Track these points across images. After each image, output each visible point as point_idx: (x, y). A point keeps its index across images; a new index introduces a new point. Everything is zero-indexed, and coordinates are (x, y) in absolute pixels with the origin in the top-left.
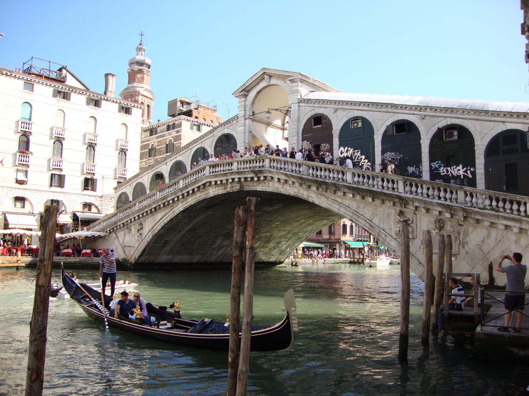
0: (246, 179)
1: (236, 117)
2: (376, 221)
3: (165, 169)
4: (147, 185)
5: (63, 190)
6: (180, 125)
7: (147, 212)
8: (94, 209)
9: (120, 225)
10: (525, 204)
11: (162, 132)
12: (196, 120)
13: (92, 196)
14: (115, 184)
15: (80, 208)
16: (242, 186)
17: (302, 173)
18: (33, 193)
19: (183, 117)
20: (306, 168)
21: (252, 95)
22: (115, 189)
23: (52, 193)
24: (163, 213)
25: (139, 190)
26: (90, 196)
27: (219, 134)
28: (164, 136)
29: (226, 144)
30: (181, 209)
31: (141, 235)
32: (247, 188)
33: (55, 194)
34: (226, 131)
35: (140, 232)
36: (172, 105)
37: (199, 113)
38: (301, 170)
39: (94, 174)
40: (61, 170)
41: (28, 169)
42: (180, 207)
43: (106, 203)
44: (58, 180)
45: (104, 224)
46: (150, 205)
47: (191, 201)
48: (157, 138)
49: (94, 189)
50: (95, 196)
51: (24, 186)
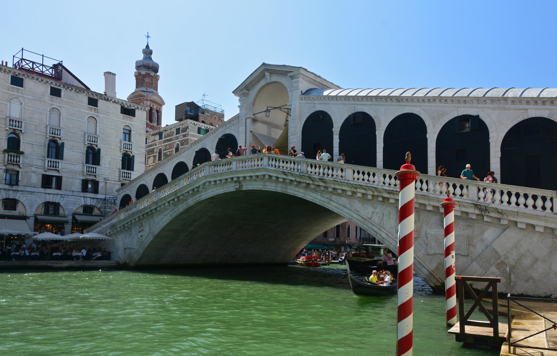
0: (245, 177)
1: (237, 117)
2: (376, 219)
3: (168, 170)
4: (150, 186)
7: (147, 213)
8: (96, 211)
9: (120, 227)
10: (551, 199)
11: (168, 136)
12: (203, 124)
13: (94, 198)
14: (118, 186)
16: (241, 186)
17: (299, 171)
18: (26, 195)
19: (189, 121)
20: (305, 165)
22: (118, 191)
23: (48, 196)
25: (142, 191)
26: (91, 198)
27: (220, 136)
28: (171, 140)
29: (227, 145)
31: (141, 236)
33: (51, 196)
34: (228, 132)
35: (140, 234)
36: (179, 108)
38: (299, 167)
39: (95, 176)
40: (58, 171)
41: (20, 171)
43: (110, 205)
45: (104, 226)
46: (149, 206)
47: (191, 202)
48: (164, 142)
49: (96, 190)
50: (97, 199)
51: (15, 188)
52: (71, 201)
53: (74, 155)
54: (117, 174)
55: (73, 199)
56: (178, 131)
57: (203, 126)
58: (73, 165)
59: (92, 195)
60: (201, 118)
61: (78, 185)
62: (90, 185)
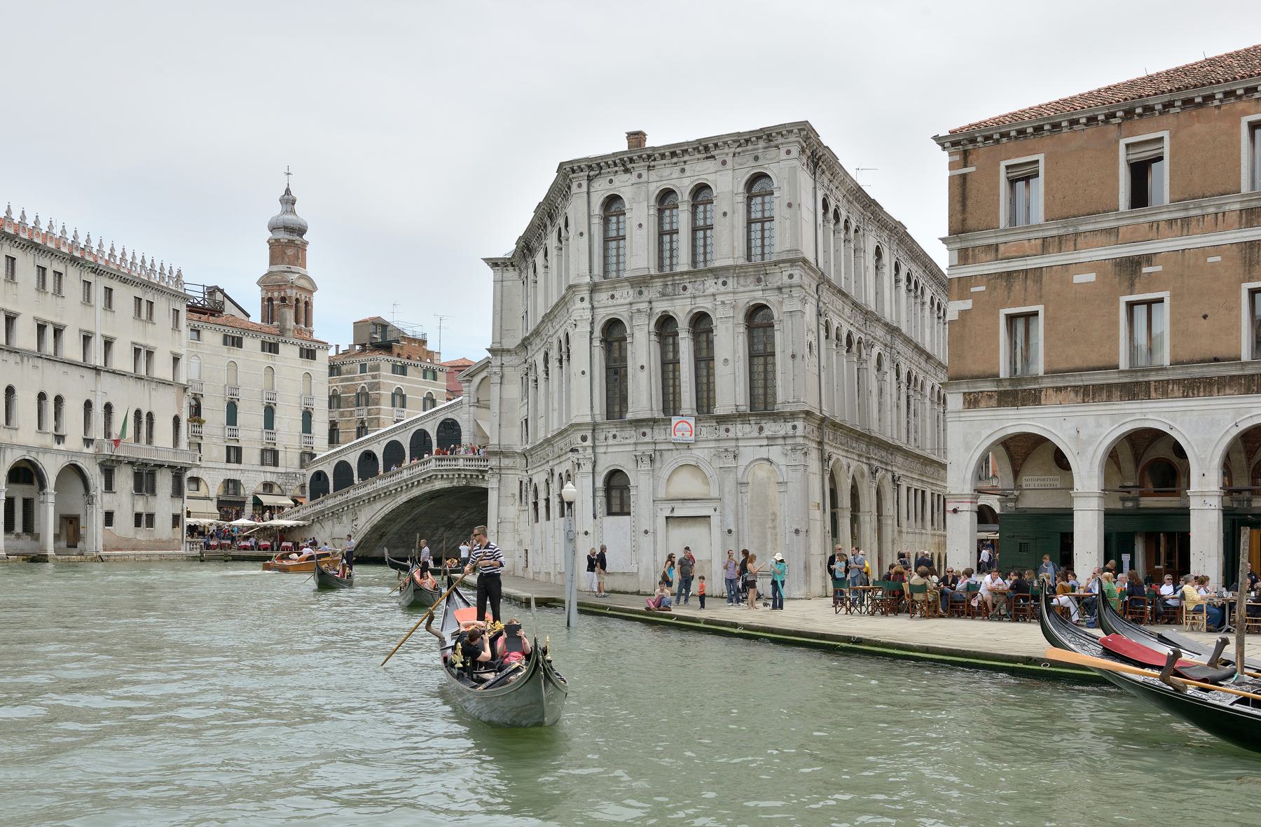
5: (241, 467)
6: (377, 368)
8: (276, 490)
11: (349, 373)
15: (261, 489)
21: (477, 380)
24: (383, 503)
27: (442, 418)
28: (352, 379)
30: (405, 500)
32: (472, 484)
34: (450, 416)
37: (402, 348)
42: (404, 498)
44: (234, 454)
47: (416, 492)
48: (342, 380)
49: (276, 464)
52: (252, 479)
53: (251, 417)
54: (298, 439)
55: (252, 475)
56: (363, 368)
57: (400, 361)
58: (251, 434)
59: (272, 469)
60: (396, 350)
61: (256, 458)
62: (270, 456)
